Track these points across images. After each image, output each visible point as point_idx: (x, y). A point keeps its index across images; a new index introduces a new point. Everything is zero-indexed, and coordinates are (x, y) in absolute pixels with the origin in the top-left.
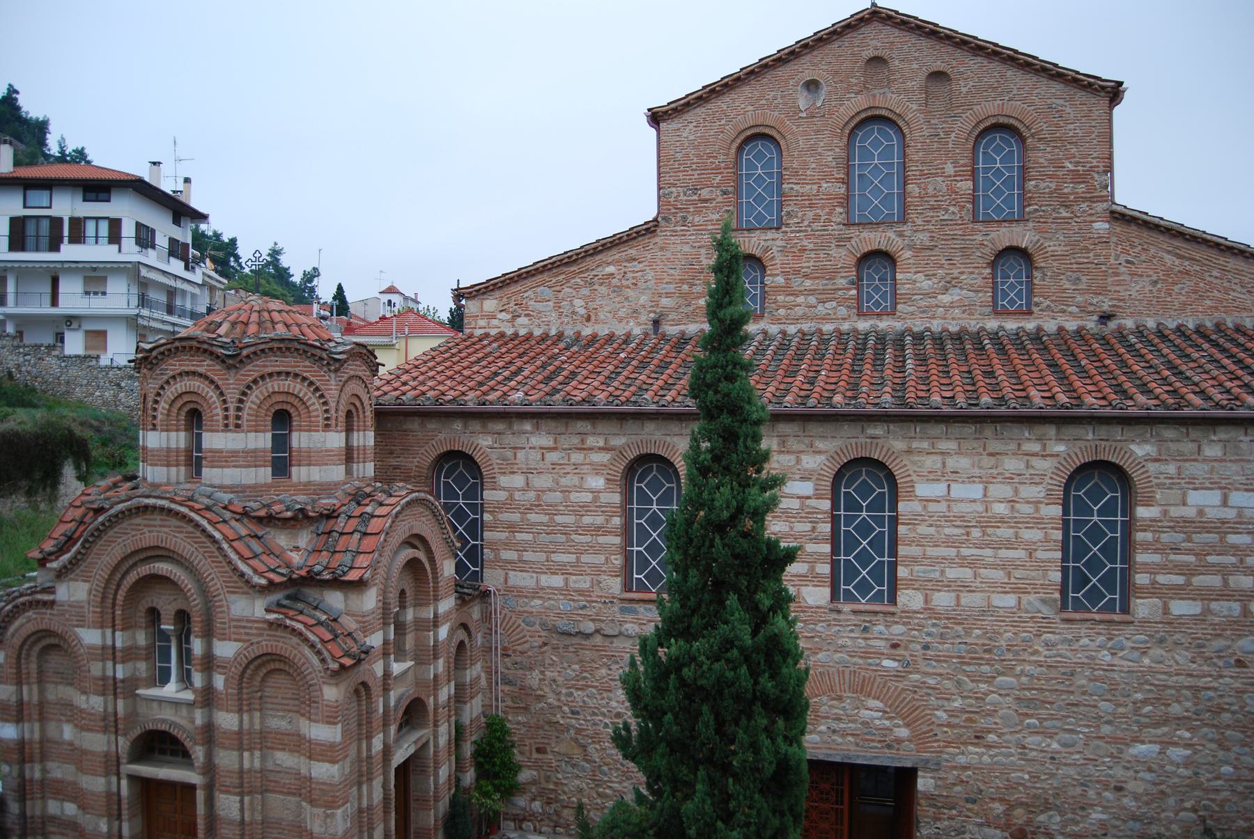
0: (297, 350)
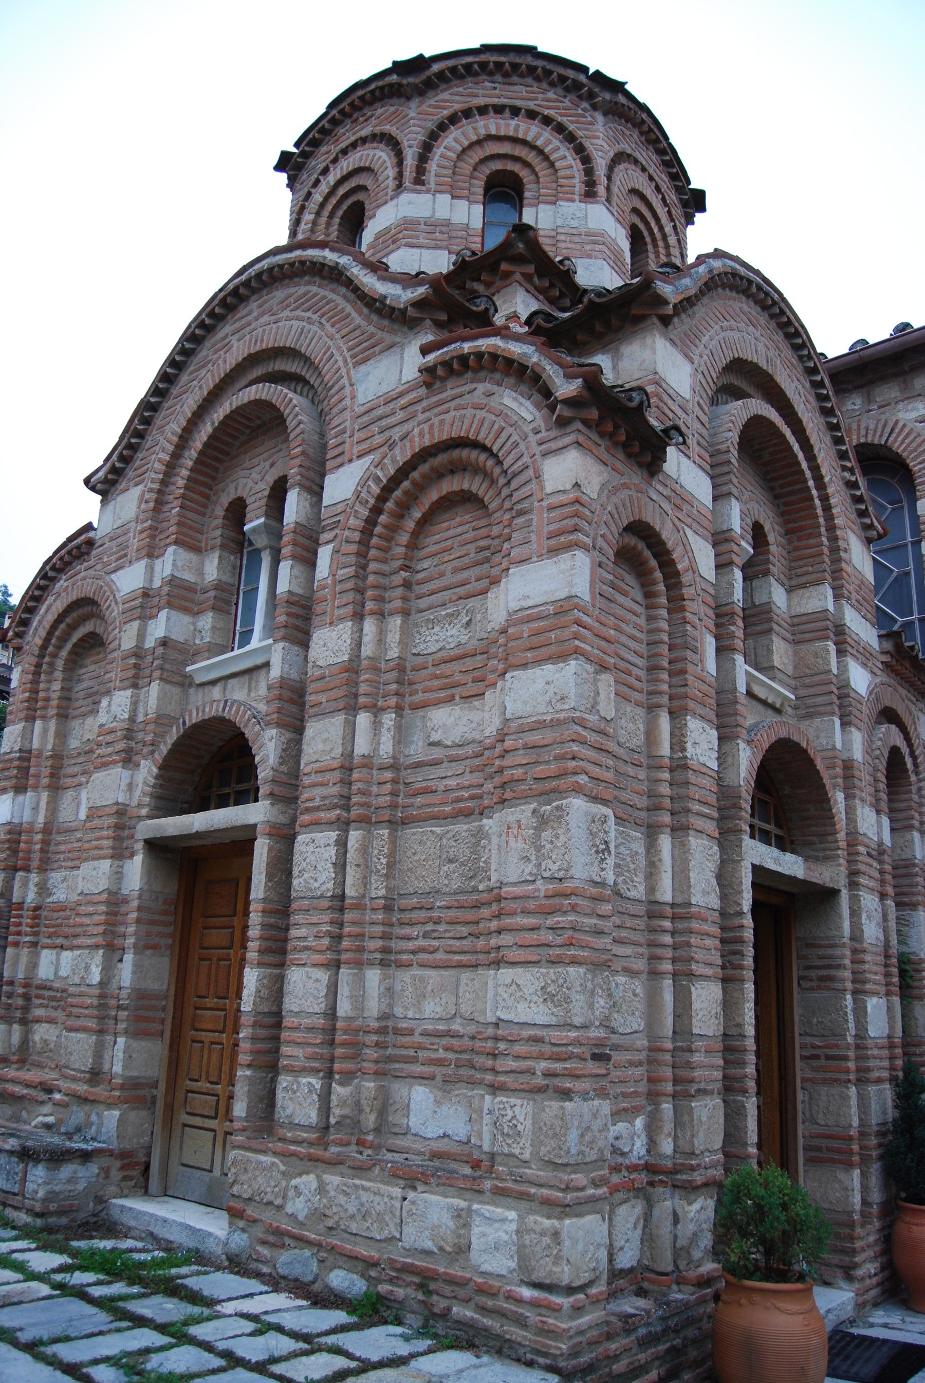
0: (531, 70)
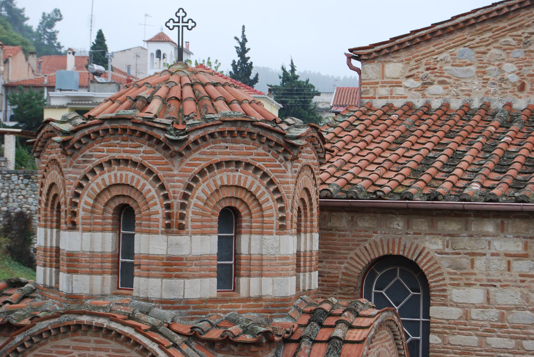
0: (250, 134)
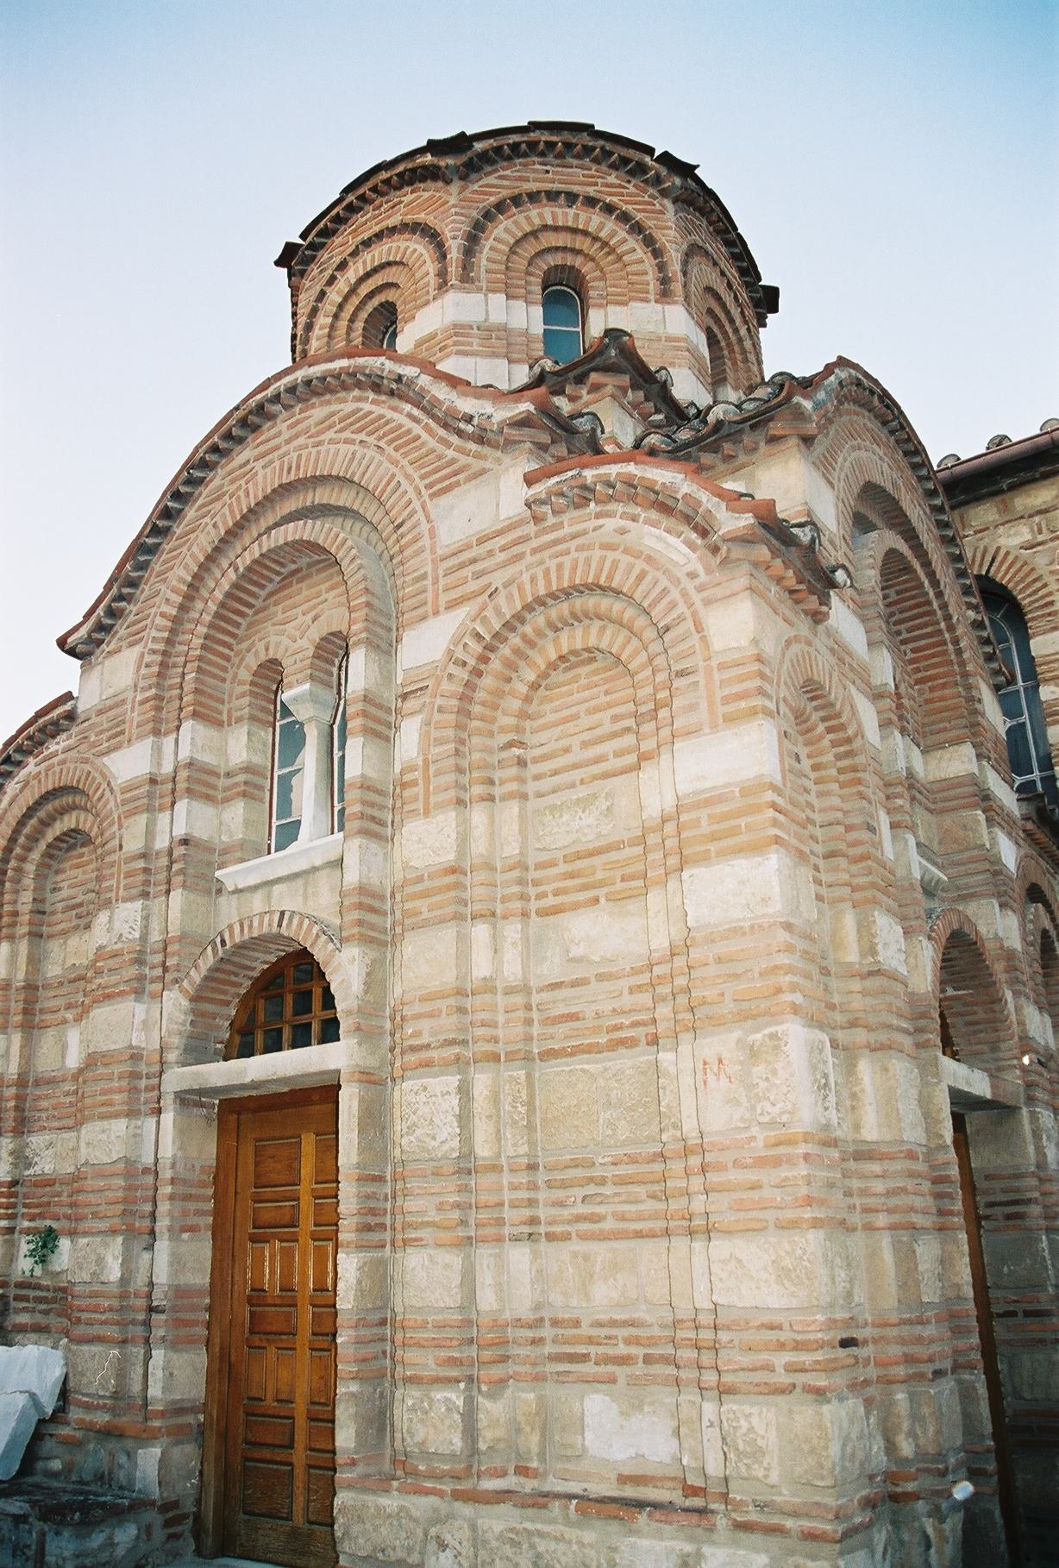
0: (587, 151)
